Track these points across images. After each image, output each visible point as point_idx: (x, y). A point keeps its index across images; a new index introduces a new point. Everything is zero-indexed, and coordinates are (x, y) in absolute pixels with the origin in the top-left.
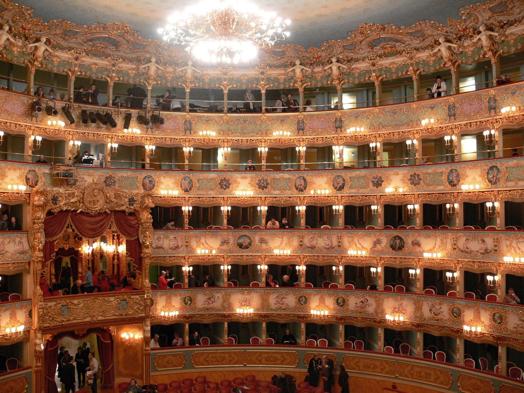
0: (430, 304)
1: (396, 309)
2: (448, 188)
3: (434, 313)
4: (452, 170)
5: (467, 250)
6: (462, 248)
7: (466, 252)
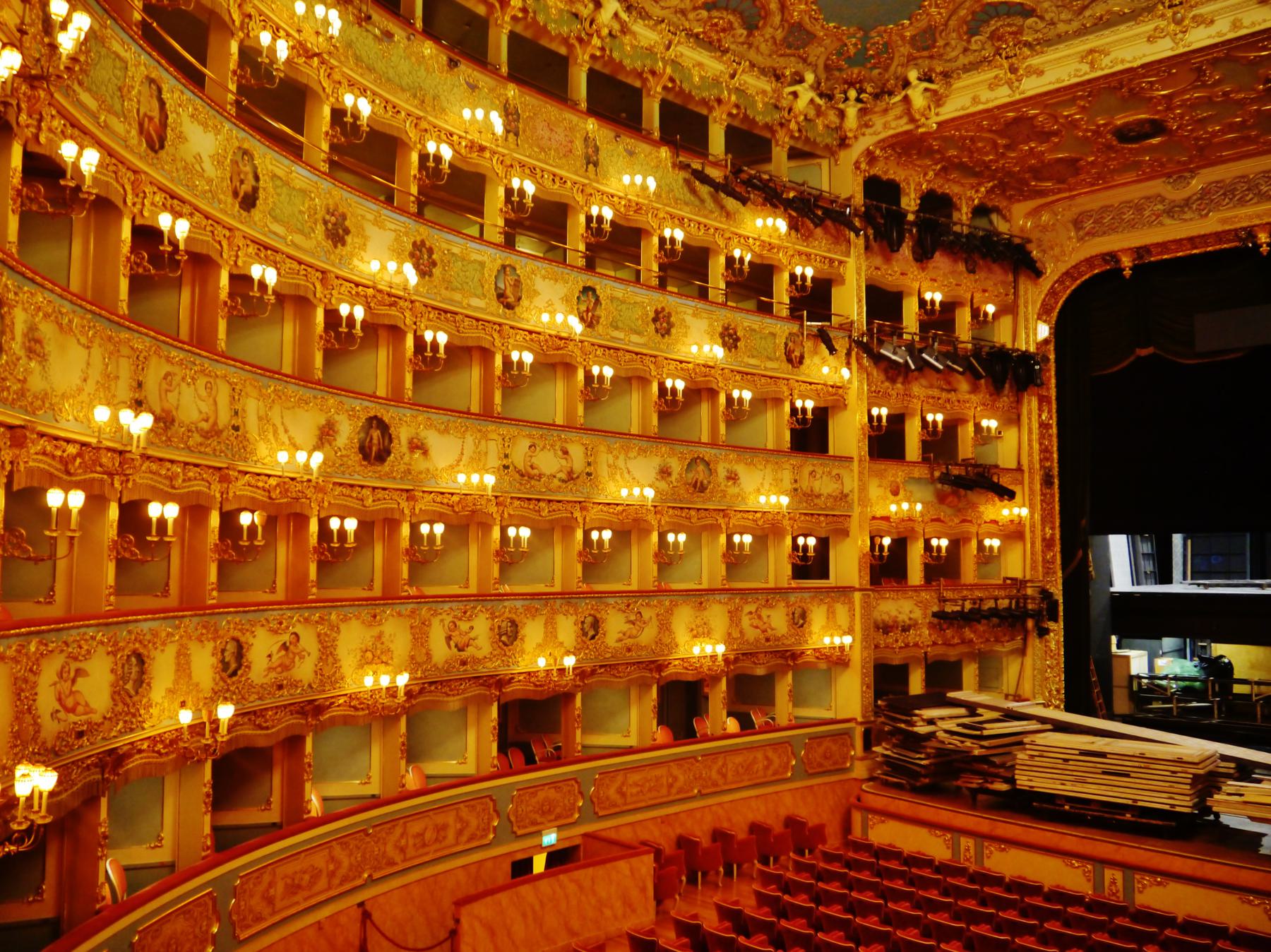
0: (446, 623)
1: (369, 655)
2: (494, 311)
3: (456, 646)
4: (504, 267)
5: (536, 472)
6: (521, 466)
7: (531, 477)
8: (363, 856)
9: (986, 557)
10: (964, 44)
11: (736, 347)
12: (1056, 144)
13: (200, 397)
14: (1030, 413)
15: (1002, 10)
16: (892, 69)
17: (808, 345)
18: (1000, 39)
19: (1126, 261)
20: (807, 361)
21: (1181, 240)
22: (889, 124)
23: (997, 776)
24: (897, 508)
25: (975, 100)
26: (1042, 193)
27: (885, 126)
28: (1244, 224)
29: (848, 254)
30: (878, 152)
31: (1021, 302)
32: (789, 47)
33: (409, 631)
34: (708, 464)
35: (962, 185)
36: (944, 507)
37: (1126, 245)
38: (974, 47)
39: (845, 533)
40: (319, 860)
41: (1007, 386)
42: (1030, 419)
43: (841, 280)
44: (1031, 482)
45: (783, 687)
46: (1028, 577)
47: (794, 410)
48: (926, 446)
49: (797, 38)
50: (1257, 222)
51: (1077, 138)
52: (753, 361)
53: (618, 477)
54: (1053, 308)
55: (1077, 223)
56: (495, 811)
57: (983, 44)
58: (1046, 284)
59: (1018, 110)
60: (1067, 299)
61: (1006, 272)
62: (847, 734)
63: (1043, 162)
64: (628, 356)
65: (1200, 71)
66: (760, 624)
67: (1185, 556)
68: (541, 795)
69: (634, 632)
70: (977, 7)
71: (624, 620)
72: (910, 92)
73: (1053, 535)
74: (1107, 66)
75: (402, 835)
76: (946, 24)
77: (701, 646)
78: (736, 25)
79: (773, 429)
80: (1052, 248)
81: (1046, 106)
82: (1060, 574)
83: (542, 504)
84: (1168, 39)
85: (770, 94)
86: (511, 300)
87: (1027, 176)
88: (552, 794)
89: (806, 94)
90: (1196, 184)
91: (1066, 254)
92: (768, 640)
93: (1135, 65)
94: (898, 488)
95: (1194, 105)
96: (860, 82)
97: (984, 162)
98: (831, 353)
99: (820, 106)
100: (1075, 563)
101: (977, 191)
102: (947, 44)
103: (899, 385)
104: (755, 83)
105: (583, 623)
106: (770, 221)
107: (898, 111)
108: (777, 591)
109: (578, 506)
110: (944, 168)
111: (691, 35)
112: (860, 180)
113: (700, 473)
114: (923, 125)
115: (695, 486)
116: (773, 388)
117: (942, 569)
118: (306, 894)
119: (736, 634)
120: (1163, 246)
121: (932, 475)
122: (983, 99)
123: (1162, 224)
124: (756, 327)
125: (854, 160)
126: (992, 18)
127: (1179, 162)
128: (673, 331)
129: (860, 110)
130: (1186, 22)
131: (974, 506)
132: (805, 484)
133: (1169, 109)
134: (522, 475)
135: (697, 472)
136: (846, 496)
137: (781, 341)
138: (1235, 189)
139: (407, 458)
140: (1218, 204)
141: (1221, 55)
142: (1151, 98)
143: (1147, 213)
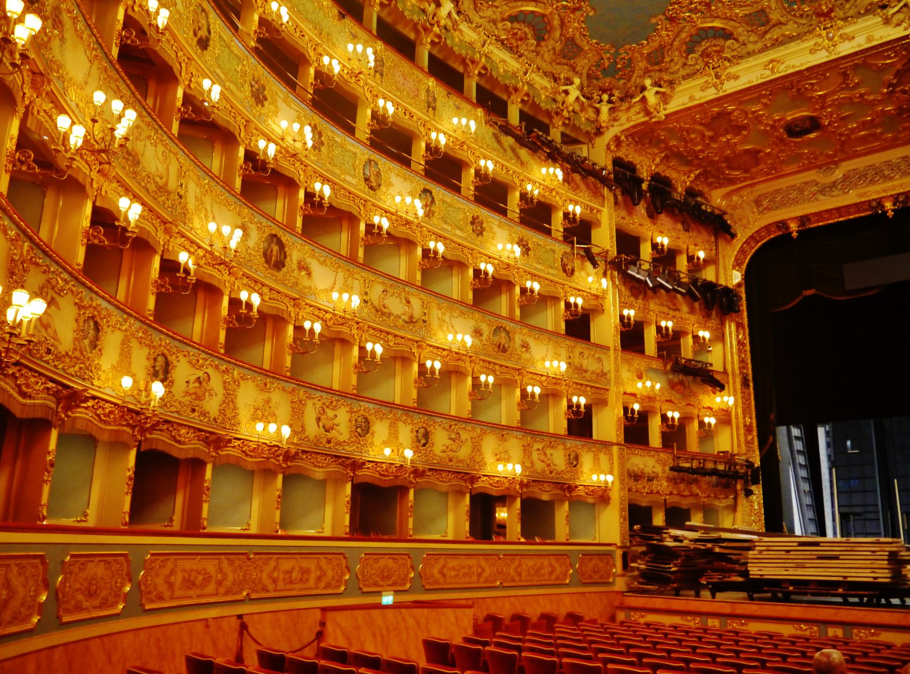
0: (318, 406)
1: (259, 412)
2: (361, 189)
3: (324, 427)
4: (370, 161)
5: (386, 310)
7: (383, 314)
8: (245, 574)
9: (706, 433)
10: (684, 60)
11: (528, 254)
12: (745, 136)
13: (158, 158)
14: (730, 334)
15: (711, 33)
16: (633, 80)
17: (577, 263)
18: (708, 56)
19: (793, 226)
20: (576, 274)
21: (832, 210)
22: (631, 118)
23: (732, 571)
24: (643, 386)
25: (692, 98)
26: (732, 181)
27: (628, 120)
28: (875, 197)
29: (603, 206)
30: (623, 138)
31: (720, 256)
32: (564, 57)
33: (290, 404)
34: (508, 333)
35: (678, 172)
36: (674, 392)
37: (793, 215)
38: (690, 62)
39: (603, 403)
40: (210, 566)
41: (714, 313)
42: (731, 337)
43: (598, 224)
44: (734, 383)
45: (562, 512)
46: (736, 452)
47: (568, 305)
48: (660, 347)
49: (570, 51)
50: (884, 195)
51: (760, 131)
52: (539, 266)
53: (445, 328)
54: (743, 263)
55: (758, 202)
56: (347, 567)
57: (696, 60)
58: (738, 244)
59: (720, 105)
60: (751, 258)
61: (710, 235)
62: (610, 555)
63: (734, 152)
64: (453, 245)
65: (845, 75)
66: (546, 460)
67: (831, 482)
68: (383, 562)
69: (454, 448)
70: (693, 31)
71: (447, 437)
72: (646, 93)
73: (751, 423)
74: (783, 70)
75: (275, 568)
76: (672, 45)
77: (505, 467)
78: (529, 36)
79: (553, 318)
80: (740, 220)
81: (741, 103)
82: (758, 453)
83: (390, 337)
84: (824, 50)
85: (550, 91)
86: (374, 184)
87: (723, 165)
88: (391, 563)
89: (574, 93)
90: (838, 174)
91: (750, 223)
92: (551, 472)
93: (803, 68)
94: (642, 374)
95: (840, 104)
96: (611, 89)
97: (695, 152)
98: (595, 267)
99: (583, 103)
100: (767, 447)
101: (688, 177)
102: (672, 60)
103: (640, 301)
104: (541, 82)
105: (417, 432)
106: (551, 170)
107: (637, 108)
108: (556, 436)
109: (416, 345)
110: (666, 157)
111: (498, 39)
112: (610, 158)
113: (502, 338)
114: (655, 117)
115: (499, 347)
116: (553, 289)
117: (674, 435)
118: (199, 592)
119: (528, 464)
120: (819, 215)
121: (665, 367)
122: (697, 97)
123: (818, 200)
124: (542, 243)
125: (606, 142)
126: (703, 40)
127: (827, 155)
128: (485, 233)
129: (610, 109)
130: (836, 39)
131: (695, 395)
132: (577, 360)
133: (823, 108)
134: (377, 311)
135: (501, 337)
136: (606, 374)
137: (558, 256)
138: (867, 174)
139: (296, 274)
140: (856, 184)
141: (860, 62)
142: (812, 98)
143: (806, 193)
